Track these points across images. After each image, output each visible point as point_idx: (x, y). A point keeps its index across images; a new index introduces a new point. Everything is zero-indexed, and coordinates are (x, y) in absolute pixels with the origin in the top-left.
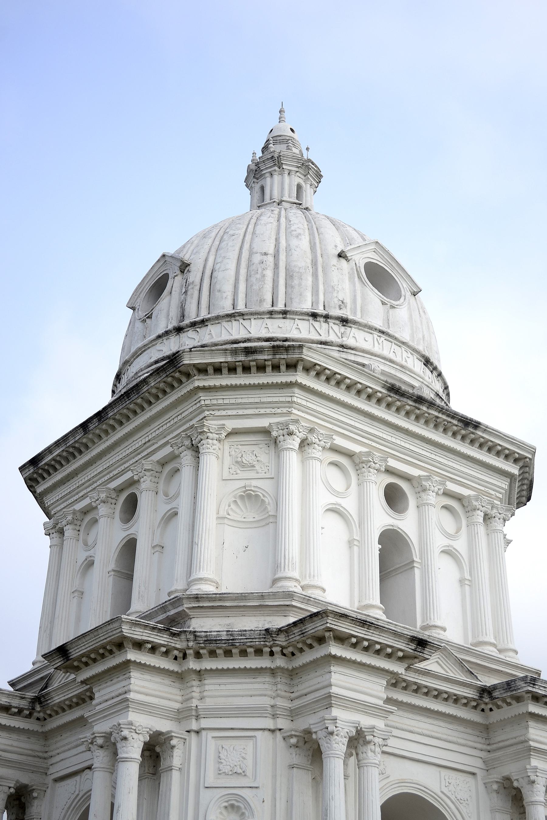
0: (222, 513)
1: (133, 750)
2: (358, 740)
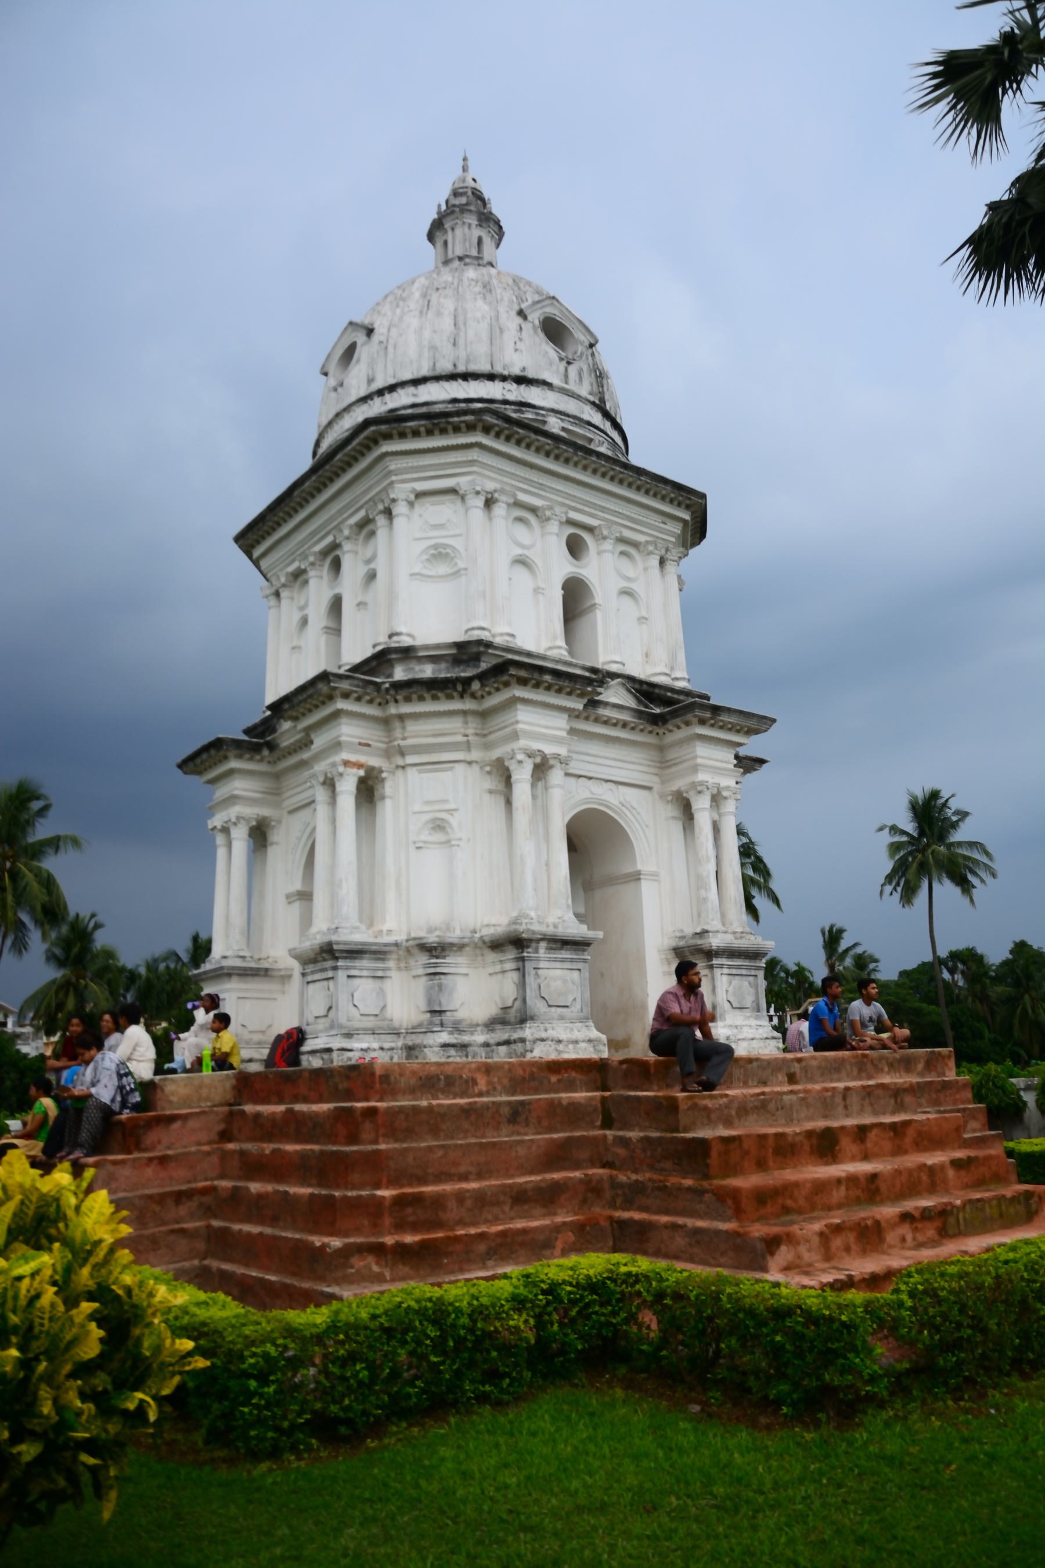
0: (416, 570)
1: (347, 787)
2: (541, 768)
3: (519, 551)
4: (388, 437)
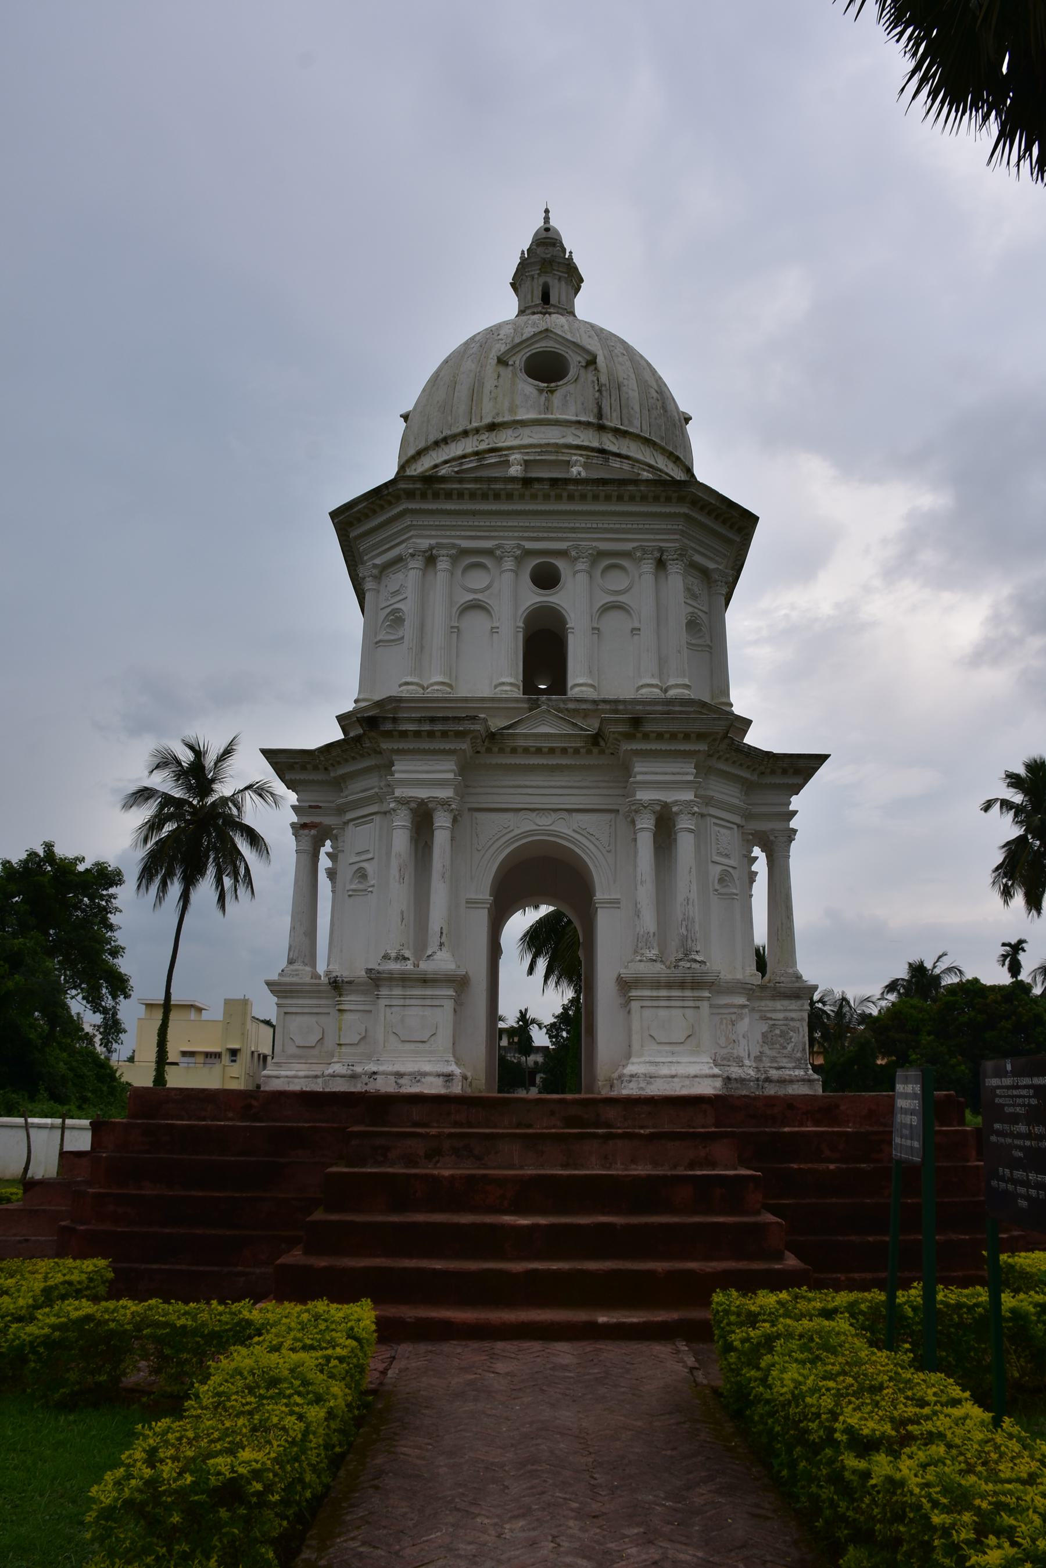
3: (471, 597)
4: (351, 524)
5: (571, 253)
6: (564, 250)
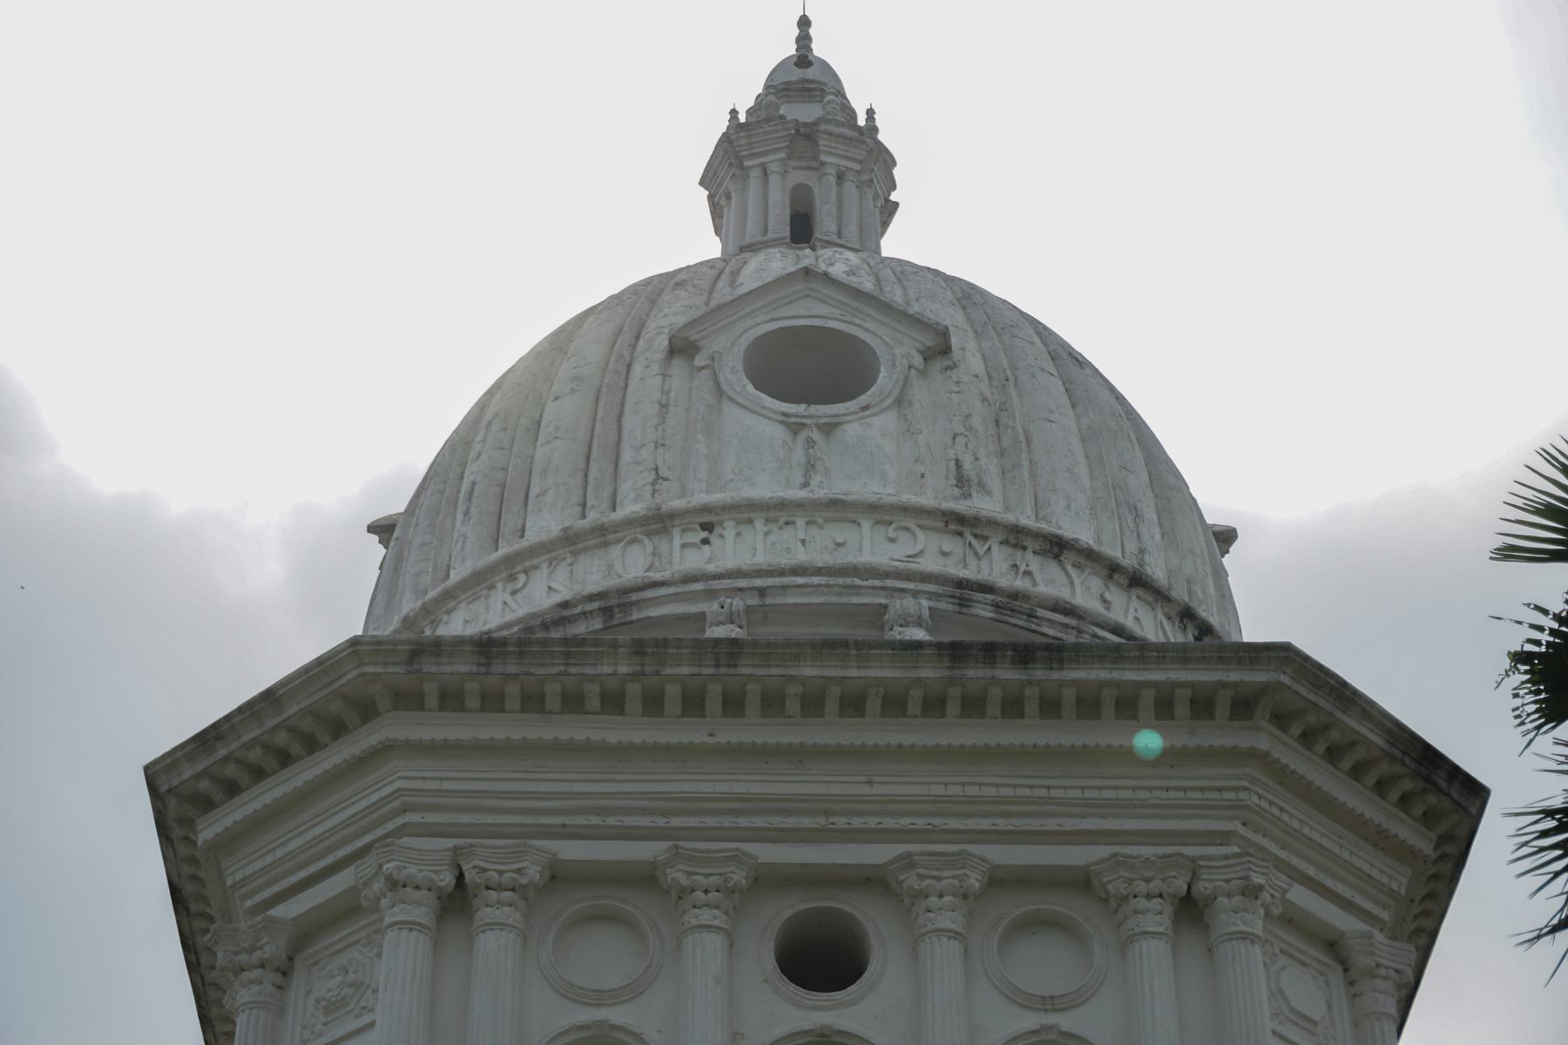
4: (206, 804)
5: (870, 113)
6: (852, 114)
